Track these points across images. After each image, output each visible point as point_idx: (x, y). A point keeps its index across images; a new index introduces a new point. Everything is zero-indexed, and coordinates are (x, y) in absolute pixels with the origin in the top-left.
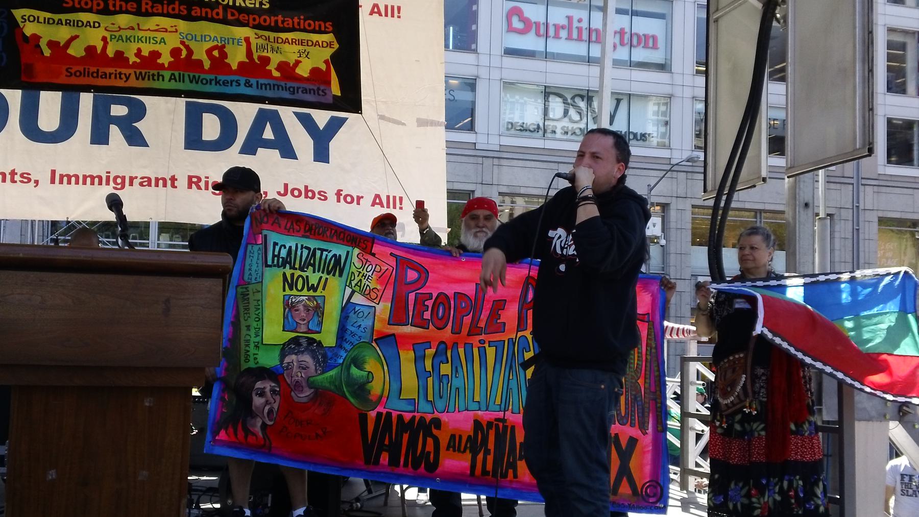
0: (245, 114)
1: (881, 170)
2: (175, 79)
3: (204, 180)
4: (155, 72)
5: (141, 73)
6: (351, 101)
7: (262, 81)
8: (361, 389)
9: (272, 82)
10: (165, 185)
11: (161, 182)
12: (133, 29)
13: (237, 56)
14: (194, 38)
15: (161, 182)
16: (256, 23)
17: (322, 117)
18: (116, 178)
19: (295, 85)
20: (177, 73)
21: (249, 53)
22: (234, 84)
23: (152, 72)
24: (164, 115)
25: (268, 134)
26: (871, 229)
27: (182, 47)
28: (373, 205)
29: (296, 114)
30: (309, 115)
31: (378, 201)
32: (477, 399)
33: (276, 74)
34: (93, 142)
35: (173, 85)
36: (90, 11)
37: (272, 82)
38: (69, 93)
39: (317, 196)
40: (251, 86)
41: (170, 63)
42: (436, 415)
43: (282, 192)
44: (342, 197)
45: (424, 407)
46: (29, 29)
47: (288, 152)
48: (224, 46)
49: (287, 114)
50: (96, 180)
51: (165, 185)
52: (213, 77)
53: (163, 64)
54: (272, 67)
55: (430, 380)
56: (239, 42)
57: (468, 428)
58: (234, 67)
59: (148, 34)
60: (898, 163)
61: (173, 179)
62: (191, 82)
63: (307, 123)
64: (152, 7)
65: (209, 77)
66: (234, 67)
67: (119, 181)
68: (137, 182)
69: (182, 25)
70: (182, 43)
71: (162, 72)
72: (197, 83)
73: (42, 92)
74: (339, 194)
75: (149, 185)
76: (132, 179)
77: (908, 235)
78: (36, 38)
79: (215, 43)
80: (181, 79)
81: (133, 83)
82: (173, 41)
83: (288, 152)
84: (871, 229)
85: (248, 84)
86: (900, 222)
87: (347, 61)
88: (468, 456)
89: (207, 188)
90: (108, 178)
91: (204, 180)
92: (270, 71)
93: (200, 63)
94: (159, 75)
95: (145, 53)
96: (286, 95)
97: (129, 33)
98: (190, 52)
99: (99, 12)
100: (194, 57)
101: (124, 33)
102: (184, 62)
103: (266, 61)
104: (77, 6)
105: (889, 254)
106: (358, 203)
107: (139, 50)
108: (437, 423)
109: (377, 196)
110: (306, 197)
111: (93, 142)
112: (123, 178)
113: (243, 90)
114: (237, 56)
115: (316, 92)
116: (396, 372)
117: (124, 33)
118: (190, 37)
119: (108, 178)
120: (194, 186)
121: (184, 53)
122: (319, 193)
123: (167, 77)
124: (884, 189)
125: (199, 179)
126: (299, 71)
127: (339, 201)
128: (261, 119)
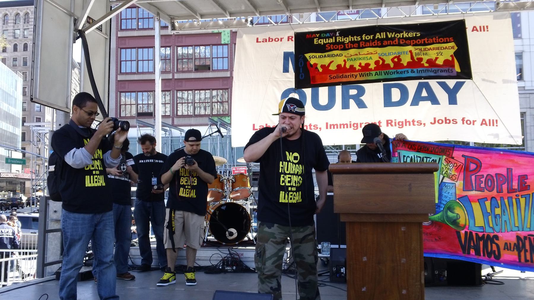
0: (412, 86)
3: (394, 121)
6: (466, 73)
7: (419, 69)
8: (455, 222)
9: (424, 69)
12: (357, 55)
13: (406, 59)
14: (385, 54)
17: (451, 83)
18: (354, 124)
20: (378, 72)
23: (367, 73)
24: (374, 92)
28: (481, 125)
29: (437, 82)
30: (444, 83)
31: (484, 122)
32: (517, 225)
33: (426, 65)
35: (377, 77)
37: (424, 69)
40: (414, 72)
41: (375, 68)
42: (495, 234)
45: (488, 230)
48: (399, 56)
49: (433, 83)
52: (395, 70)
54: (424, 62)
55: (490, 217)
57: (514, 240)
58: (405, 64)
59: (364, 56)
65: (393, 71)
66: (405, 64)
69: (379, 50)
70: (380, 58)
71: (371, 72)
73: (320, 88)
79: (395, 55)
81: (359, 78)
82: (376, 58)
85: (413, 72)
88: (516, 252)
89: (395, 125)
91: (394, 121)
92: (423, 64)
93: (388, 65)
96: (432, 74)
97: (355, 57)
98: (384, 61)
99: (341, 50)
100: (386, 63)
101: (353, 57)
102: (381, 66)
103: (421, 59)
104: (332, 48)
106: (473, 124)
107: (360, 64)
108: (497, 237)
109: (484, 120)
114: (406, 59)
116: (471, 213)
117: (353, 57)
120: (389, 125)
121: (381, 62)
123: (374, 74)
125: (392, 121)
128: (420, 87)
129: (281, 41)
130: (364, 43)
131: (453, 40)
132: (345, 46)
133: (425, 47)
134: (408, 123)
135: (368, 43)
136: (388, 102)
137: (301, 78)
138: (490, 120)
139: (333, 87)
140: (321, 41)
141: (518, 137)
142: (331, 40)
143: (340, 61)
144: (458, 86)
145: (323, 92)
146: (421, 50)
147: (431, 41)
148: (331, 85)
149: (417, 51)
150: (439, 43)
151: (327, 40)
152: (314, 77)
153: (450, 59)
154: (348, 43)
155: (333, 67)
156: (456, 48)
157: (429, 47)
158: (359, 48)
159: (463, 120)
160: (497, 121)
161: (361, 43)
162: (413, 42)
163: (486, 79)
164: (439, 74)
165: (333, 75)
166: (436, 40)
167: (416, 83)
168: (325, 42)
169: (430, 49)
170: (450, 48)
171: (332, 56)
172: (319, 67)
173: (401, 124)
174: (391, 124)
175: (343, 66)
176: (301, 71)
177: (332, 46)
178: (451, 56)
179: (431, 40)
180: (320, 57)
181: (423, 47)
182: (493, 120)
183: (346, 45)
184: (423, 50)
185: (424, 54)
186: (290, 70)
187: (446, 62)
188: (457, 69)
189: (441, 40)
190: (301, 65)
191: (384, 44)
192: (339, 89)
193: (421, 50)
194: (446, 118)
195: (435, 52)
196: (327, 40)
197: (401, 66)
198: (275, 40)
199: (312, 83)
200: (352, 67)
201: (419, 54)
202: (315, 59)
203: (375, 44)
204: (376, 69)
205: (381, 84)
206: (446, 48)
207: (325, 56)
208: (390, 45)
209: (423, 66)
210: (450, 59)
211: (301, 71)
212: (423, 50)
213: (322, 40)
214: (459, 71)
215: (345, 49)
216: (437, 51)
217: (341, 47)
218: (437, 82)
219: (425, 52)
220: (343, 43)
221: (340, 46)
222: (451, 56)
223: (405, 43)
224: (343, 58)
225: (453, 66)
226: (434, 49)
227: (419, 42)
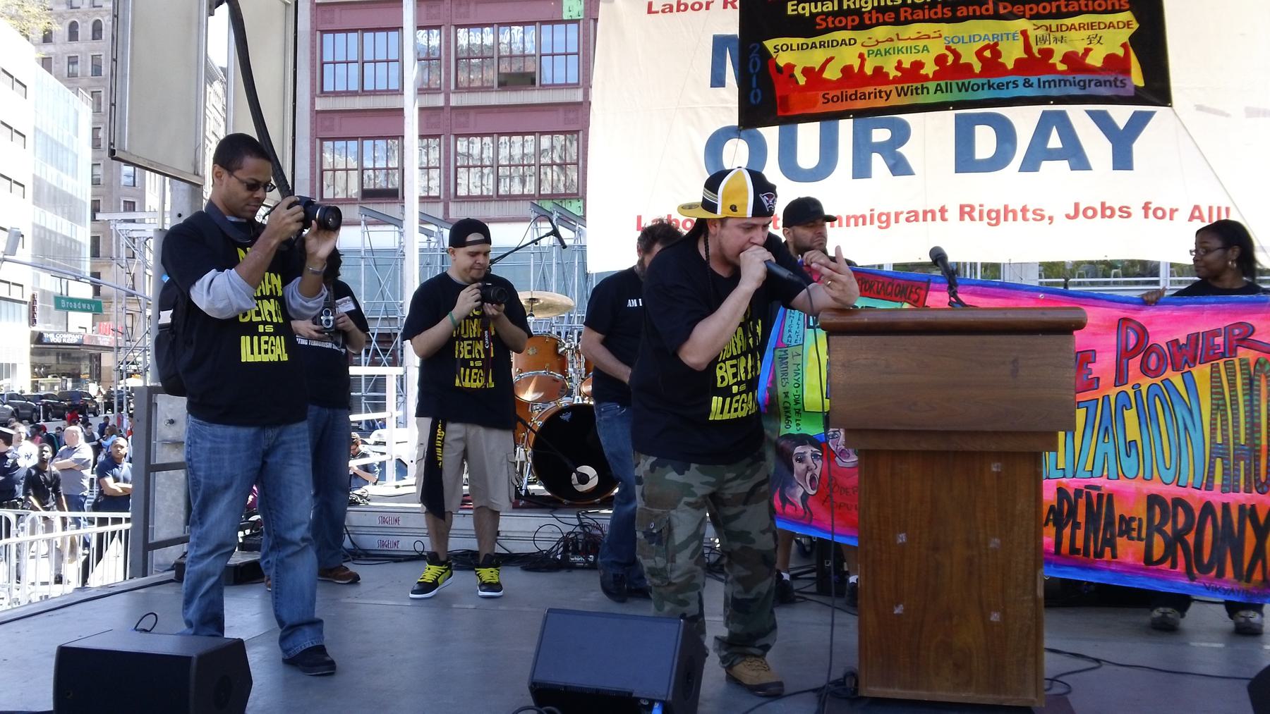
0: (1025, 120)
3: (977, 209)
4: (919, 85)
7: (1044, 78)
10: (933, 219)
11: (929, 215)
12: (891, 40)
13: (1012, 53)
14: (961, 40)
15: (929, 215)
17: (1121, 114)
19: (1086, 77)
20: (943, 83)
21: (1027, 48)
22: (1011, 85)
24: (931, 133)
25: (1055, 142)
27: (947, 53)
29: (1088, 112)
30: (1105, 113)
31: (1197, 214)
33: (1062, 67)
36: (845, 28)
38: (826, 123)
39: (1118, 213)
40: (1031, 86)
41: (935, 73)
43: (1072, 214)
44: (1151, 212)
46: (782, 59)
48: (996, 44)
49: (1077, 114)
50: (861, 220)
51: (933, 219)
52: (984, 80)
53: (927, 75)
54: (1056, 60)
56: (1012, 37)
58: (1010, 66)
59: (909, 43)
61: (943, 210)
62: (960, 90)
63: (1104, 122)
64: (912, 14)
66: (1010, 66)
67: (884, 218)
68: (902, 218)
69: (946, 29)
70: (948, 48)
71: (925, 84)
73: (800, 126)
74: (1146, 207)
75: (916, 220)
76: (897, 215)
78: (790, 67)
79: (987, 42)
80: (949, 89)
81: (895, 101)
82: (938, 48)
85: (1027, 84)
87: (1150, 43)
89: (981, 219)
90: (872, 216)
91: (977, 209)
92: (1054, 65)
93: (969, 67)
95: (906, 65)
96: (1075, 91)
97: (888, 45)
98: (957, 56)
99: (854, 28)
100: (962, 61)
101: (882, 47)
102: (951, 69)
103: (1048, 53)
104: (831, 26)
106: (1171, 219)
107: (900, 63)
110: (1103, 216)
112: (888, 215)
114: (1012, 53)
115: (1113, 84)
117: (882, 47)
118: (956, 40)
119: (872, 216)
121: (951, 59)
122: (1120, 209)
123: (932, 90)
125: (972, 208)
127: (1146, 216)
129: (707, 8)
130: (910, 11)
131: (1128, 6)
132: (862, 19)
133: (1059, 22)
135: (920, 12)
137: (753, 101)
139: (832, 123)
140: (804, 9)
142: (830, 4)
143: (849, 56)
144: (1138, 123)
145: (809, 134)
146: (1049, 29)
148: (828, 118)
149: (1041, 32)
150: (1094, 12)
151: (819, 4)
152: (785, 100)
153: (1121, 52)
154: (870, 12)
155: (833, 73)
156: (1135, 26)
157: (1068, 21)
158: (897, 22)
161: (902, 10)
162: (1031, 9)
165: (832, 93)
166: (1087, 6)
167: (1036, 112)
168: (814, 11)
169: (1072, 28)
170: (1121, 25)
171: (832, 44)
172: (798, 73)
173: (993, 215)
174: (970, 214)
175: (856, 70)
176: (754, 85)
177: (830, 19)
178: (1124, 45)
179: (1076, 5)
180: (801, 47)
181: (1054, 23)
183: (866, 17)
184: (1054, 28)
185: (1056, 39)
186: (727, 81)
187: (1110, 59)
188: (1137, 78)
190: (754, 67)
191: (959, 14)
192: (846, 127)
193: (1049, 29)
195: (1085, 33)
196: (819, 4)
197: (1000, 70)
198: (693, 8)
199: (780, 113)
200: (878, 70)
201: (1044, 40)
202: (789, 53)
203: (936, 13)
204: (937, 75)
205: (949, 116)
206: (1111, 26)
207: (814, 46)
208: (974, 17)
209: (1052, 69)
210: (1121, 52)
211: (754, 85)
212: (1054, 28)
213: (807, 5)
214: (1141, 83)
215: (862, 26)
216: (1091, 32)
217: (853, 21)
218: (1088, 112)
219: (1059, 35)
220: (858, 12)
221: (849, 19)
222: (1124, 45)
223: (1011, 12)
224: (858, 49)
225: (1127, 71)
226: (1081, 27)
227: (1044, 8)
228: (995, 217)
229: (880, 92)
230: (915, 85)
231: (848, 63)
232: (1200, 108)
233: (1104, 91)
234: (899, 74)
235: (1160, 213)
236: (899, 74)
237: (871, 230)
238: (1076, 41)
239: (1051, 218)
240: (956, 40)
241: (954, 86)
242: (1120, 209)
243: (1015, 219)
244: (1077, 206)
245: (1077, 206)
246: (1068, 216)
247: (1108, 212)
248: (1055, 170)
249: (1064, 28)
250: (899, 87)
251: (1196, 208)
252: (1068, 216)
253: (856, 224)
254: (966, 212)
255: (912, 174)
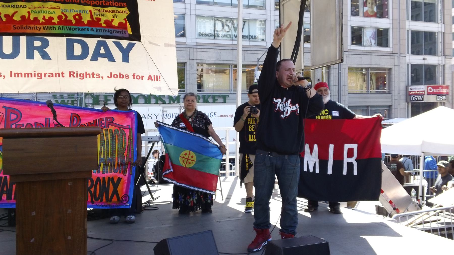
0: (92, 43)
1: (349, 48)
2: (60, 29)
4: (52, 26)
5: (45, 27)
7: (98, 28)
9: (102, 29)
12: (41, 8)
13: (86, 18)
16: (94, 4)
17: (125, 43)
20: (61, 26)
22: (86, 30)
24: (57, 45)
25: (102, 51)
26: (345, 72)
27: (62, 15)
29: (114, 42)
30: (119, 42)
34: (27, 58)
35: (60, 32)
37: (102, 29)
38: (15, 37)
40: (93, 31)
41: (58, 22)
47: (111, 58)
48: (80, 14)
49: (110, 42)
52: (77, 27)
53: (55, 23)
54: (102, 22)
56: (87, 12)
58: (86, 23)
59: (47, 10)
60: (356, 44)
62: (68, 30)
63: (119, 46)
65: (75, 27)
66: (86, 23)
70: (63, 13)
71: (55, 26)
72: (70, 30)
73: (3, 37)
77: (360, 73)
79: (77, 13)
80: (63, 29)
81: (42, 31)
82: (59, 13)
83: (111, 58)
84: (345, 72)
85: (92, 30)
86: (357, 68)
92: (101, 24)
93: (71, 21)
94: (53, 28)
95: (47, 18)
96: (109, 34)
97: (39, 9)
98: (66, 17)
100: (68, 19)
101: (37, 10)
102: (64, 21)
103: (99, 20)
105: (352, 82)
107: (44, 17)
111: (27, 58)
113: (90, 32)
114: (86, 18)
117: (37, 10)
118: (65, 11)
121: (64, 17)
122: (126, 76)
123: (57, 29)
124: (350, 56)
126: (113, 24)
128: (99, 45)
134: (88, 76)
136: (71, 56)
138: (154, 76)
141: (175, 90)
143: (24, 12)
144: (130, 47)
146: (99, 10)
147: (108, 3)
149: (96, 12)
153: (124, 22)
155: (17, 18)
157: (106, 9)
159: (134, 75)
160: (160, 77)
163: (152, 42)
164: (115, 34)
165: (17, 26)
171: (16, 6)
175: (27, 18)
178: (125, 19)
181: (101, 9)
182: (157, 76)
184: (101, 11)
185: (102, 15)
187: (120, 23)
188: (129, 31)
189: (117, 4)
193: (99, 10)
194: (120, 73)
197: (82, 24)
200: (36, 19)
201: (97, 14)
204: (59, 23)
207: (9, 6)
210: (124, 22)
212: (101, 11)
214: (131, 33)
216: (113, 14)
218: (114, 42)
219: (103, 13)
222: (125, 19)
224: (27, 10)
225: (126, 29)
226: (110, 11)
228: (83, 76)
229: (37, 27)
230: (50, 26)
231: (23, 15)
232: (150, 43)
233: (118, 35)
234: (44, 21)
235: (138, 77)
236: (44, 21)
237: (35, 79)
238: (109, 16)
239: (102, 77)
240: (65, 11)
241: (65, 28)
242: (126, 76)
243: (90, 77)
244: (111, 73)
245: (111, 73)
246: (108, 77)
247: (122, 76)
248: (103, 61)
249: (104, 11)
250: (44, 26)
251: (150, 76)
252: (108, 77)
253: (28, 77)
254: (71, 74)
255: (50, 59)
